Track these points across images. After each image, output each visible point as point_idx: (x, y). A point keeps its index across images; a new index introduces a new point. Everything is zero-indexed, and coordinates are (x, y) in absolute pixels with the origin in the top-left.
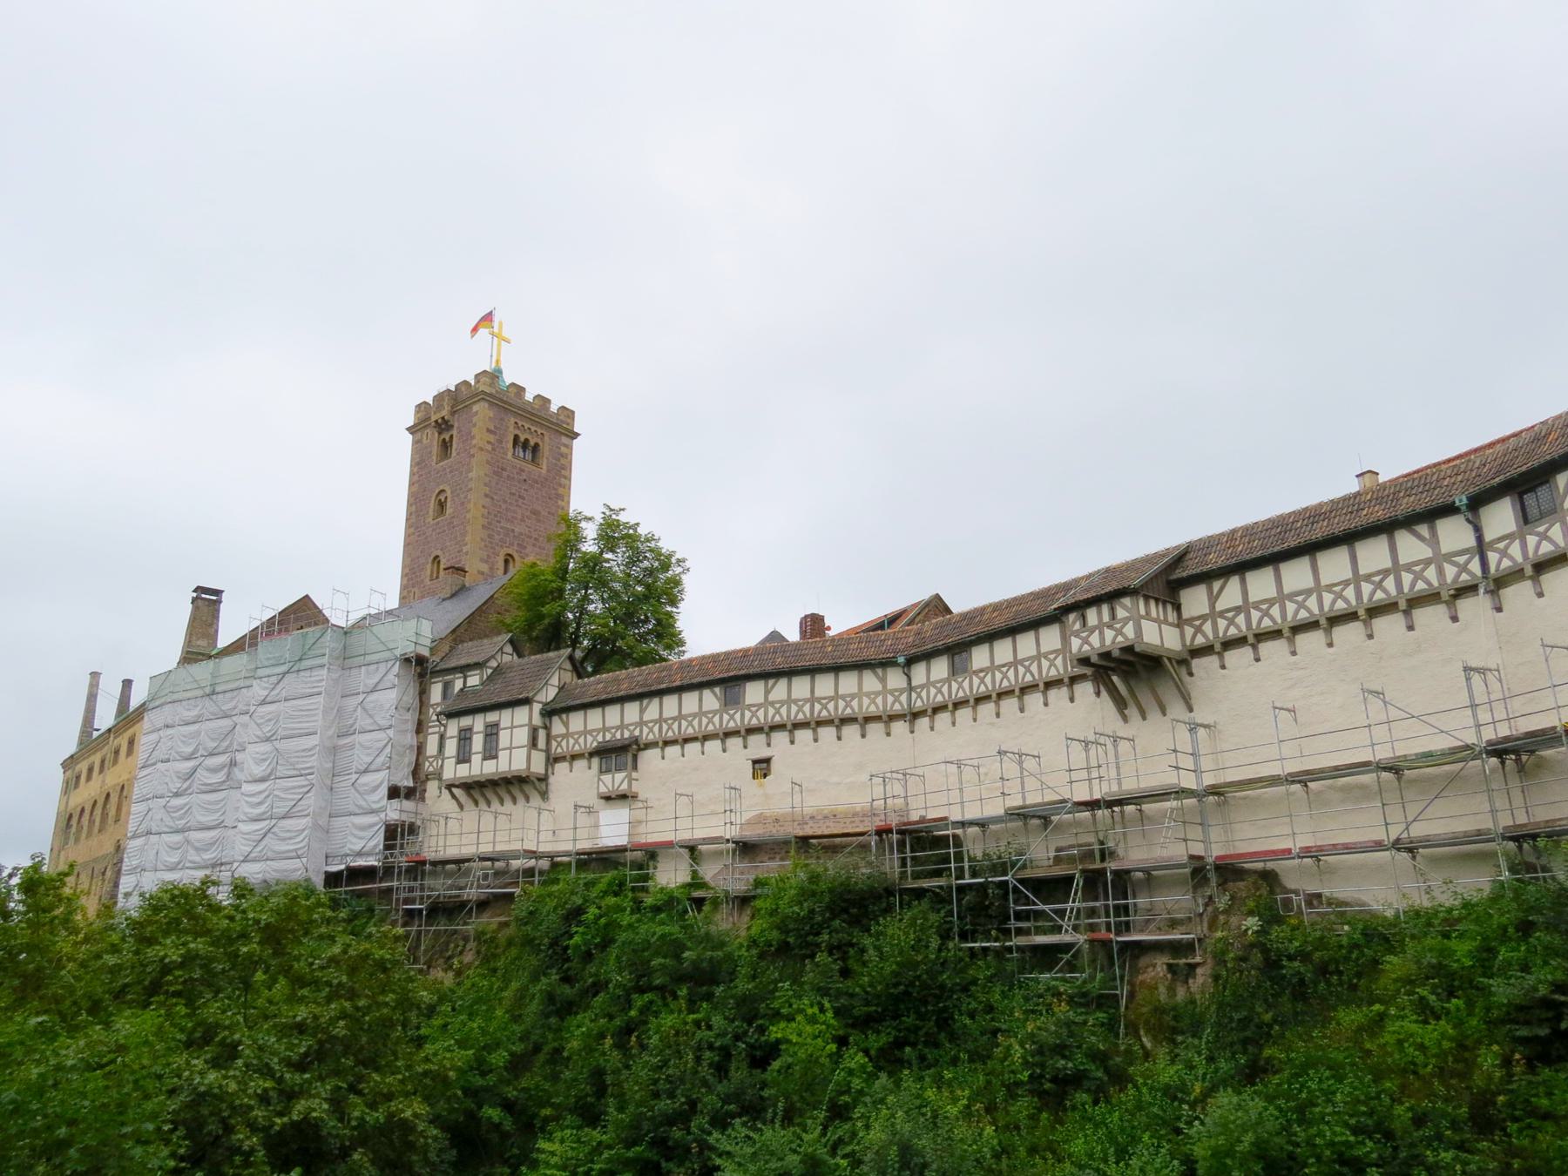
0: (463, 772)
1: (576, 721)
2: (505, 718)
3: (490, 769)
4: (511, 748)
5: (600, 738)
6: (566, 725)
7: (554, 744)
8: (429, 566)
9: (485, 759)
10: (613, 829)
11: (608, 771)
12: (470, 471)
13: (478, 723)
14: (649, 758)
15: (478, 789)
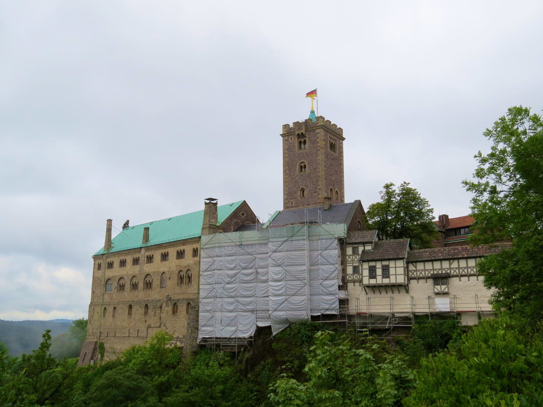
0: (373, 282)
1: (420, 266)
2: (392, 264)
3: (386, 281)
4: (396, 275)
5: (432, 272)
6: (416, 267)
7: (410, 274)
8: (299, 192)
9: (383, 277)
10: (442, 305)
11: (438, 284)
12: (317, 156)
13: (379, 265)
14: (454, 281)
15: (375, 288)
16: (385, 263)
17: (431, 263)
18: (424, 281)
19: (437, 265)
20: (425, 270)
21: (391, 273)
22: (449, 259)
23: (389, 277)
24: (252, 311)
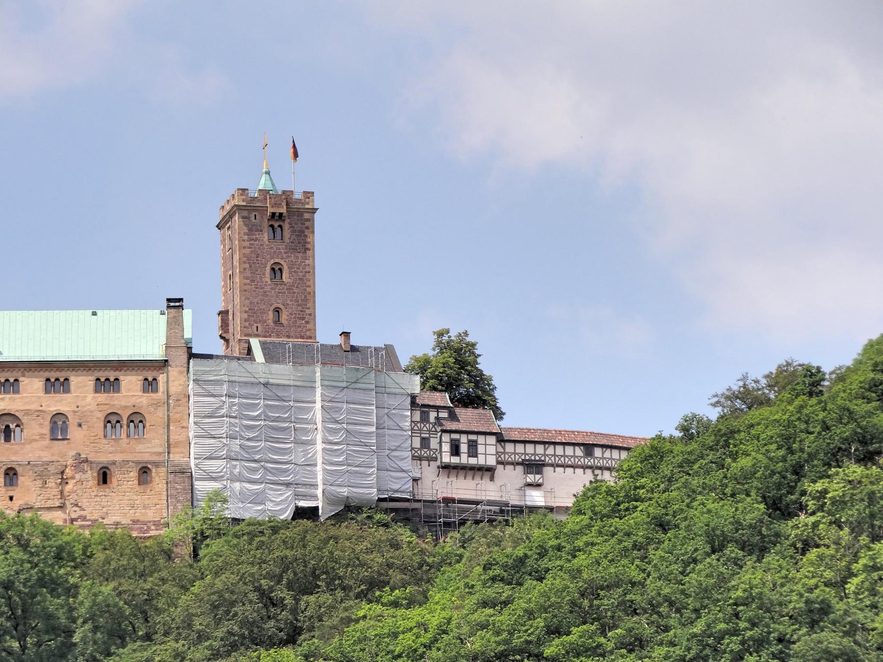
0: (455, 460)
2: (481, 439)
3: (473, 461)
4: (485, 454)
5: (523, 457)
6: (504, 448)
9: (469, 456)
13: (464, 439)
16: (473, 437)
17: (523, 445)
18: (512, 467)
19: (530, 448)
20: (515, 453)
21: (479, 452)
22: (544, 443)
23: (476, 456)
24: (288, 485)
